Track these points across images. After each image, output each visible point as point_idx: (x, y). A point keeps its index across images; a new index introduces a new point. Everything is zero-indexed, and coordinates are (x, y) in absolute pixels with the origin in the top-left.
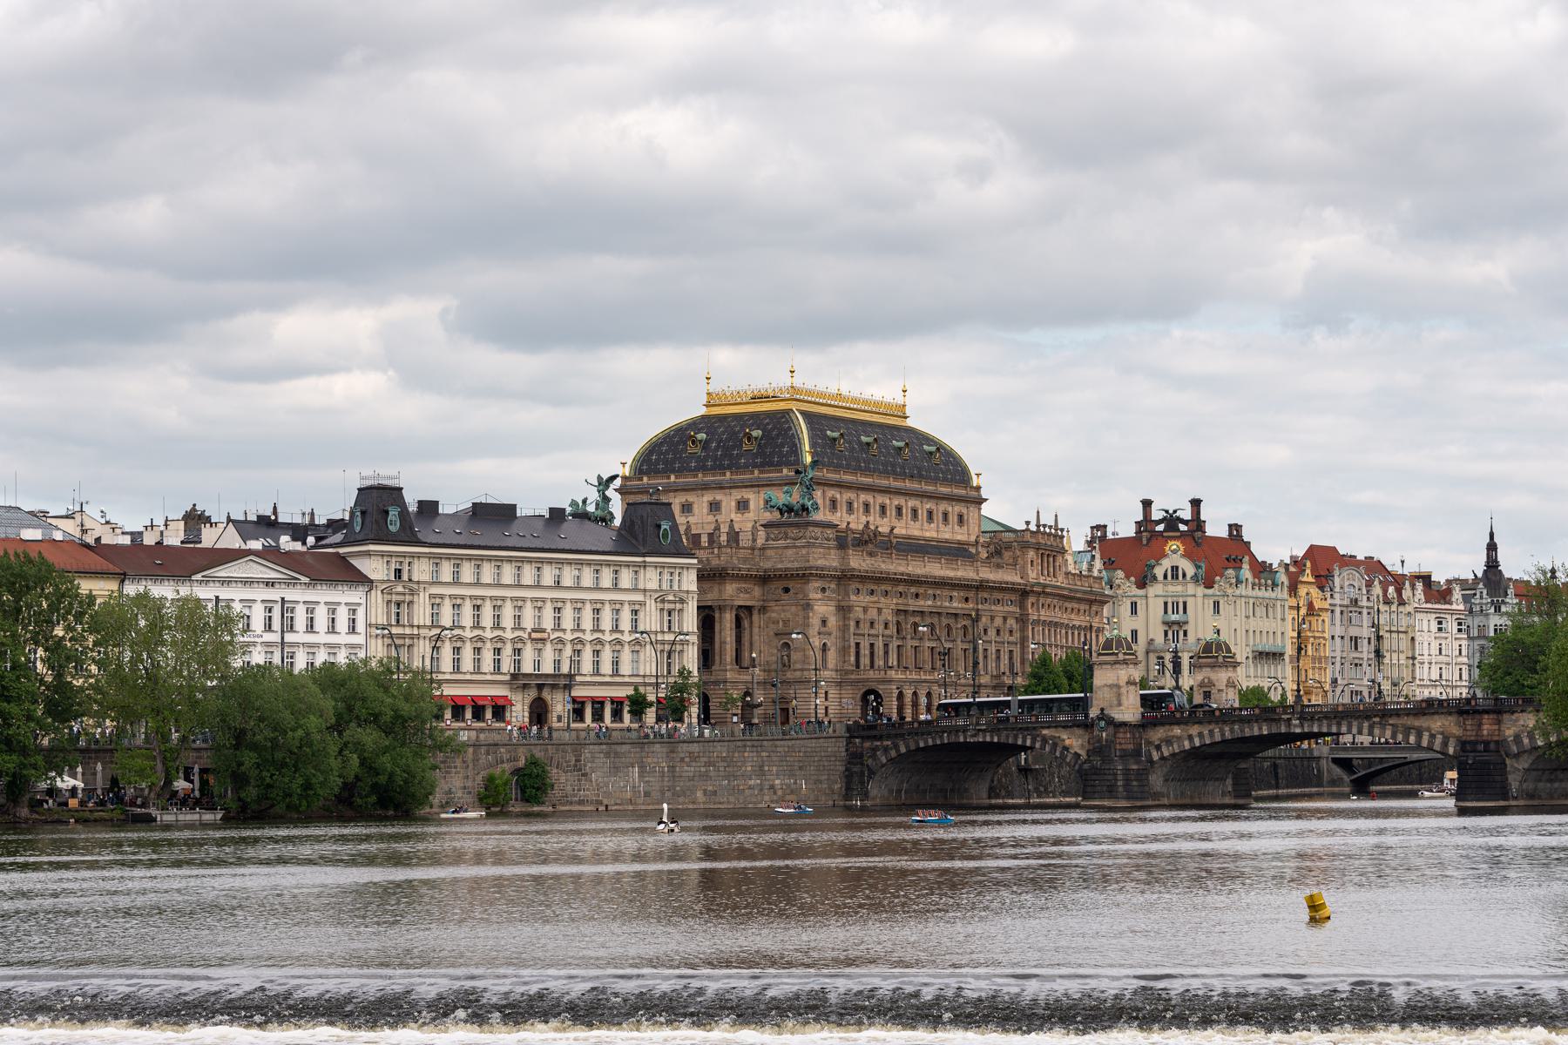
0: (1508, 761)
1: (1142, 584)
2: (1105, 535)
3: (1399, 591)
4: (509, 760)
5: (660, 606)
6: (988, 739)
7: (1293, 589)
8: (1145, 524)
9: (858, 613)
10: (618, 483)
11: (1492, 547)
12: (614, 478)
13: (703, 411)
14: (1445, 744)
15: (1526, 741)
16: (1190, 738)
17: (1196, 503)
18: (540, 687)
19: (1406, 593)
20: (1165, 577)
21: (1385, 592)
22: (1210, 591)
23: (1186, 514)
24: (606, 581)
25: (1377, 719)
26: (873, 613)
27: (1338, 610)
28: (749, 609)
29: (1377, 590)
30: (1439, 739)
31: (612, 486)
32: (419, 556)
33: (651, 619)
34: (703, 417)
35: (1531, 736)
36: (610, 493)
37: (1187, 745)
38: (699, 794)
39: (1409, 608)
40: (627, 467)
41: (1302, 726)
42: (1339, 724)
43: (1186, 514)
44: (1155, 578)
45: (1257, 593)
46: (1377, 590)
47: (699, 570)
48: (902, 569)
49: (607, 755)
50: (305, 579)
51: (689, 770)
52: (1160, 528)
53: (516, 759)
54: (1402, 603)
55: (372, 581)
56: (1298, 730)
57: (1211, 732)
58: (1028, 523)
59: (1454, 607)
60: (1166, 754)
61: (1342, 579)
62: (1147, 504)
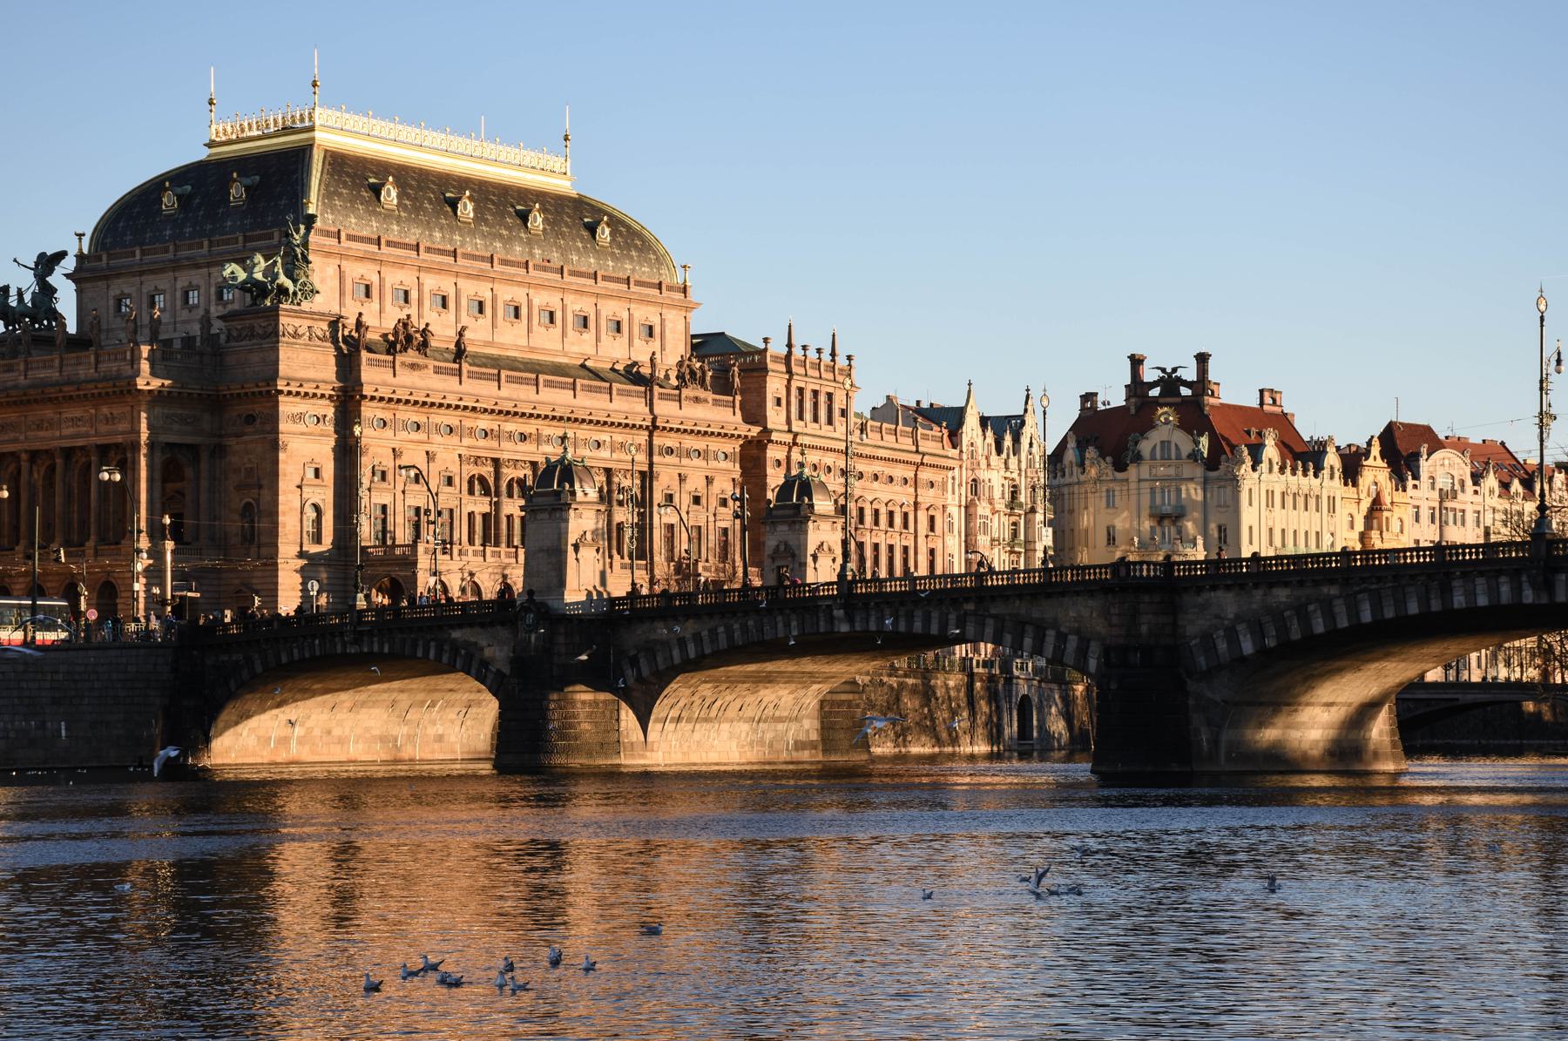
0: (1192, 686)
1: (1120, 467)
2: (1094, 403)
8: (1137, 387)
10: (69, 264)
12: (62, 255)
13: (202, 154)
14: (1082, 653)
15: (1222, 646)
16: (682, 642)
17: (1202, 359)
20: (1153, 457)
21: (1505, 486)
22: (1212, 474)
23: (1190, 374)
25: (970, 607)
28: (193, 449)
29: (1491, 481)
30: (1073, 642)
35: (1232, 637)
40: (86, 241)
41: (850, 619)
42: (910, 618)
43: (1190, 374)
44: (1138, 458)
46: (1491, 481)
52: (1155, 392)
56: (845, 628)
57: (713, 633)
58: (766, 340)
61: (1441, 467)
62: (1136, 362)
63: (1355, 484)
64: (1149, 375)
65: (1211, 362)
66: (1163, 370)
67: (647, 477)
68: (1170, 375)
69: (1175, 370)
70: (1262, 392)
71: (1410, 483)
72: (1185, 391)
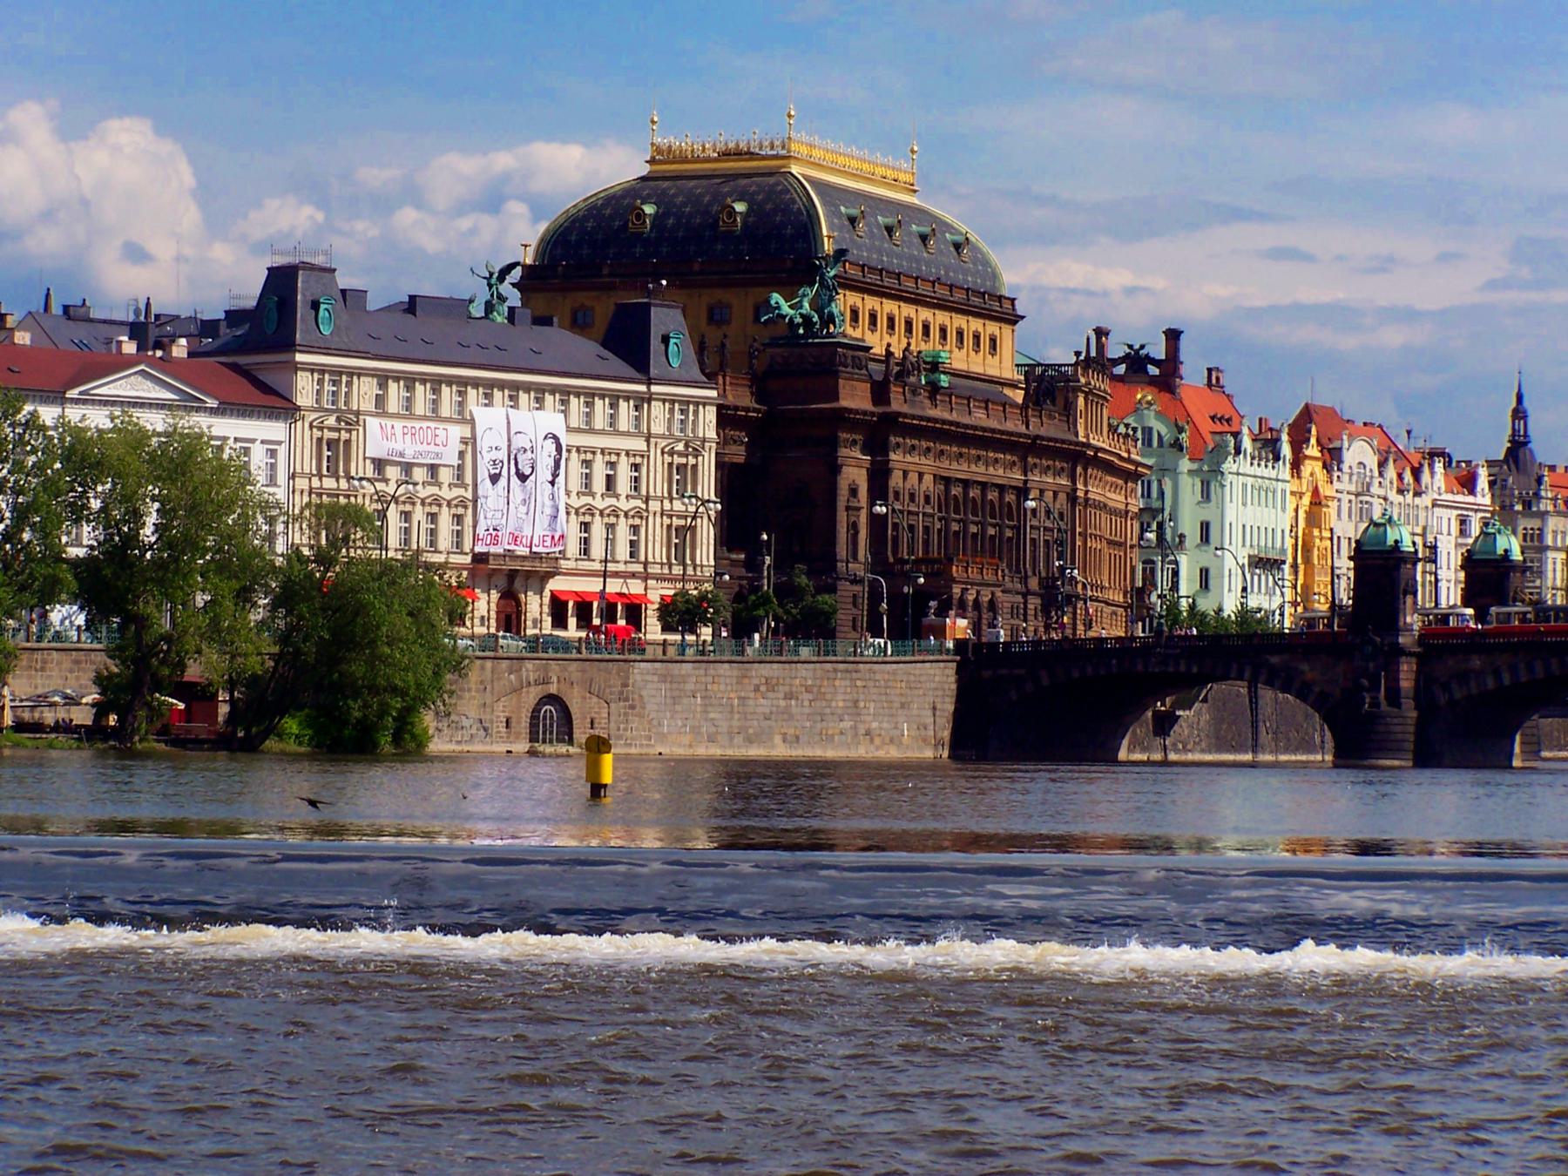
3: (1416, 473)
4: (537, 683)
5: (668, 459)
6: (1183, 668)
7: (1296, 466)
9: (896, 480)
10: (517, 274)
11: (1519, 414)
13: (645, 170)
16: (1497, 673)
17: (1173, 336)
18: (512, 575)
19: (1426, 477)
21: (1400, 477)
23: (1159, 351)
24: (600, 421)
26: (913, 477)
27: (1345, 498)
29: (1391, 472)
31: (509, 279)
32: (361, 373)
33: (656, 480)
34: (643, 179)
36: (506, 288)
37: (1491, 683)
38: (778, 739)
39: (1425, 500)
40: (531, 251)
43: (1159, 351)
45: (1256, 470)
46: (1391, 472)
47: (720, 408)
48: (946, 416)
49: (664, 678)
50: (212, 403)
51: (763, 706)
53: (546, 682)
54: (1417, 494)
55: (298, 409)
59: (1479, 500)
60: (1458, 695)
62: (1100, 333)
63: (1299, 477)
64: (1115, 350)
65: (1184, 342)
66: (1130, 347)
67: (1023, 492)
68: (1137, 352)
69: (1142, 347)
70: (1210, 370)
71: (1336, 474)
72: (1153, 370)
